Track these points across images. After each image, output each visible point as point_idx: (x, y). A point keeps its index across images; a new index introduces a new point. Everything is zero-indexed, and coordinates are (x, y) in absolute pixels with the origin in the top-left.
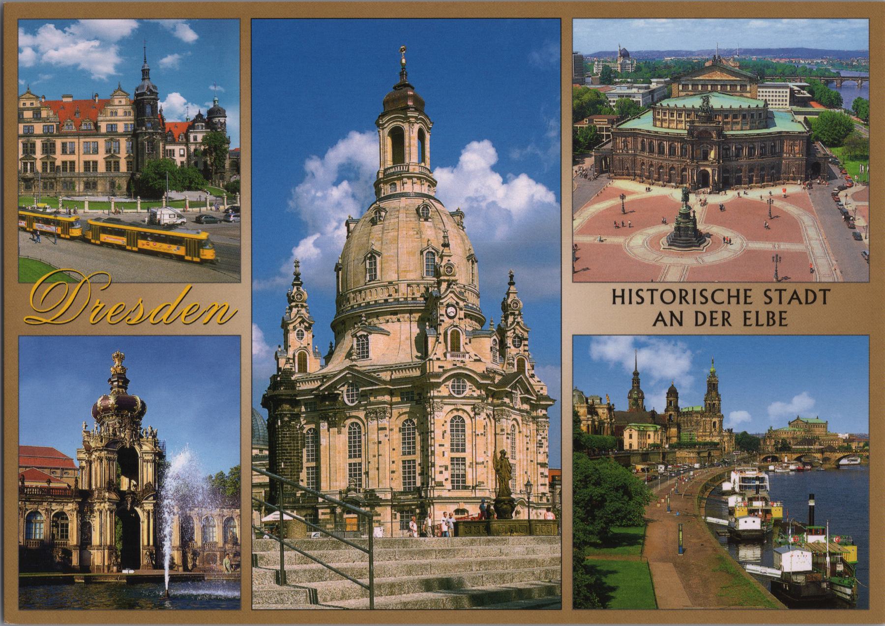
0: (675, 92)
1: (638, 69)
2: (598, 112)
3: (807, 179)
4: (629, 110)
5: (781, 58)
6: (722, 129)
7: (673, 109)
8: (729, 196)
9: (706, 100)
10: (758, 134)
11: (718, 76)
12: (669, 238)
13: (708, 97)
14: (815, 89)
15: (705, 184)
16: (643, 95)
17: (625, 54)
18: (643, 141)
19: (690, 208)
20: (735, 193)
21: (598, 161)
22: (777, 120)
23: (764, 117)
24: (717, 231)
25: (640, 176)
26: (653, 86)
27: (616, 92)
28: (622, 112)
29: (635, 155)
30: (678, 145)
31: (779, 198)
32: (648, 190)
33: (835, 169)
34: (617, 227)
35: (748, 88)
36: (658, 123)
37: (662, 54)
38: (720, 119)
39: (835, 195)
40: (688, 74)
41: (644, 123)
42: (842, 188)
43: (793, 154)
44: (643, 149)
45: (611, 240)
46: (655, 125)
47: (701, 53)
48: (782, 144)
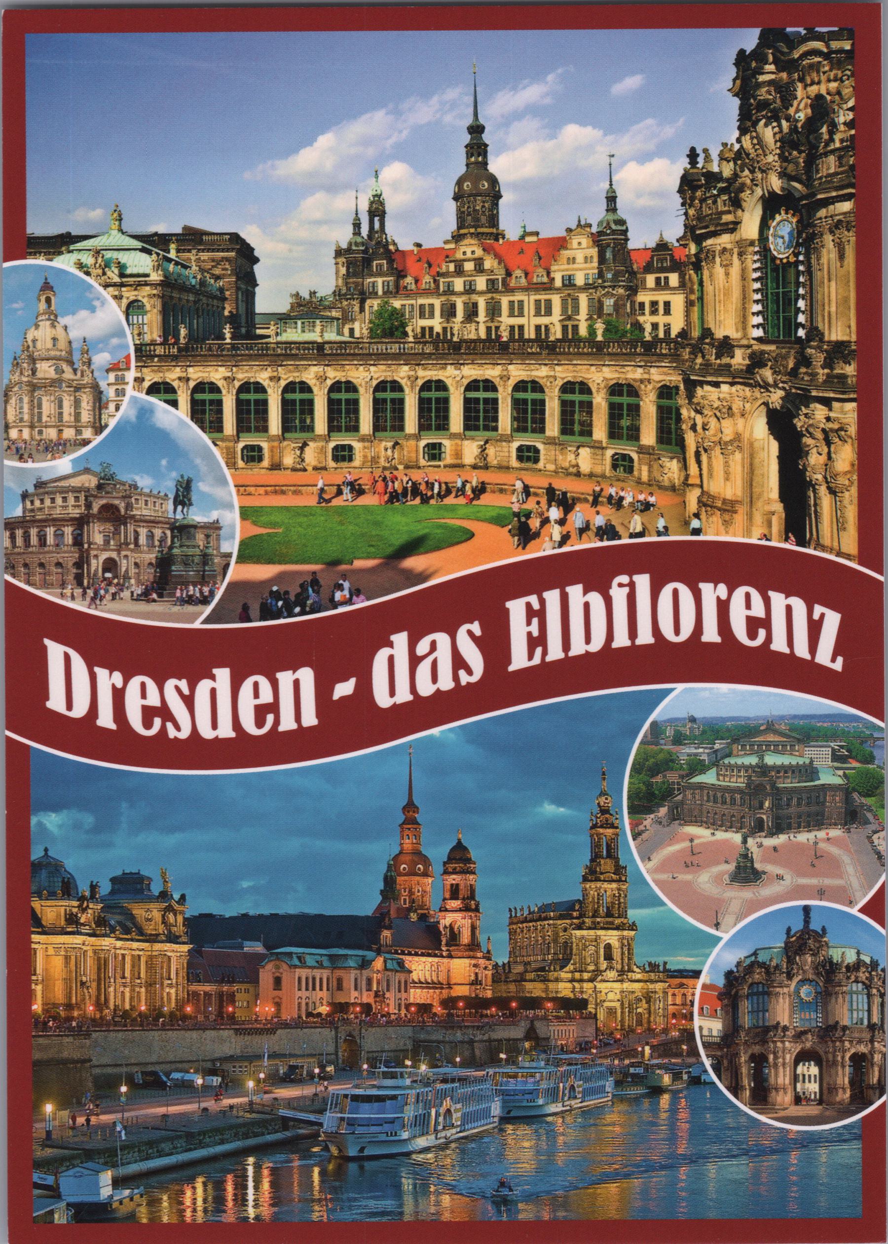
0: (735, 752)
1: (704, 732)
3: (846, 824)
4: (698, 767)
7: (733, 766)
8: (781, 839)
9: (762, 758)
10: (805, 787)
11: (771, 738)
14: (852, 747)
15: (761, 829)
17: (693, 720)
19: (748, 850)
20: (786, 836)
21: (671, 810)
22: (821, 775)
23: (810, 771)
25: (706, 823)
26: (717, 746)
27: (685, 752)
28: (690, 769)
29: (701, 805)
31: (823, 840)
33: (869, 816)
34: (687, 866)
35: (797, 748)
36: (721, 778)
38: (773, 774)
39: (869, 838)
40: (745, 737)
41: (709, 778)
42: (875, 832)
43: (834, 803)
47: (757, 718)
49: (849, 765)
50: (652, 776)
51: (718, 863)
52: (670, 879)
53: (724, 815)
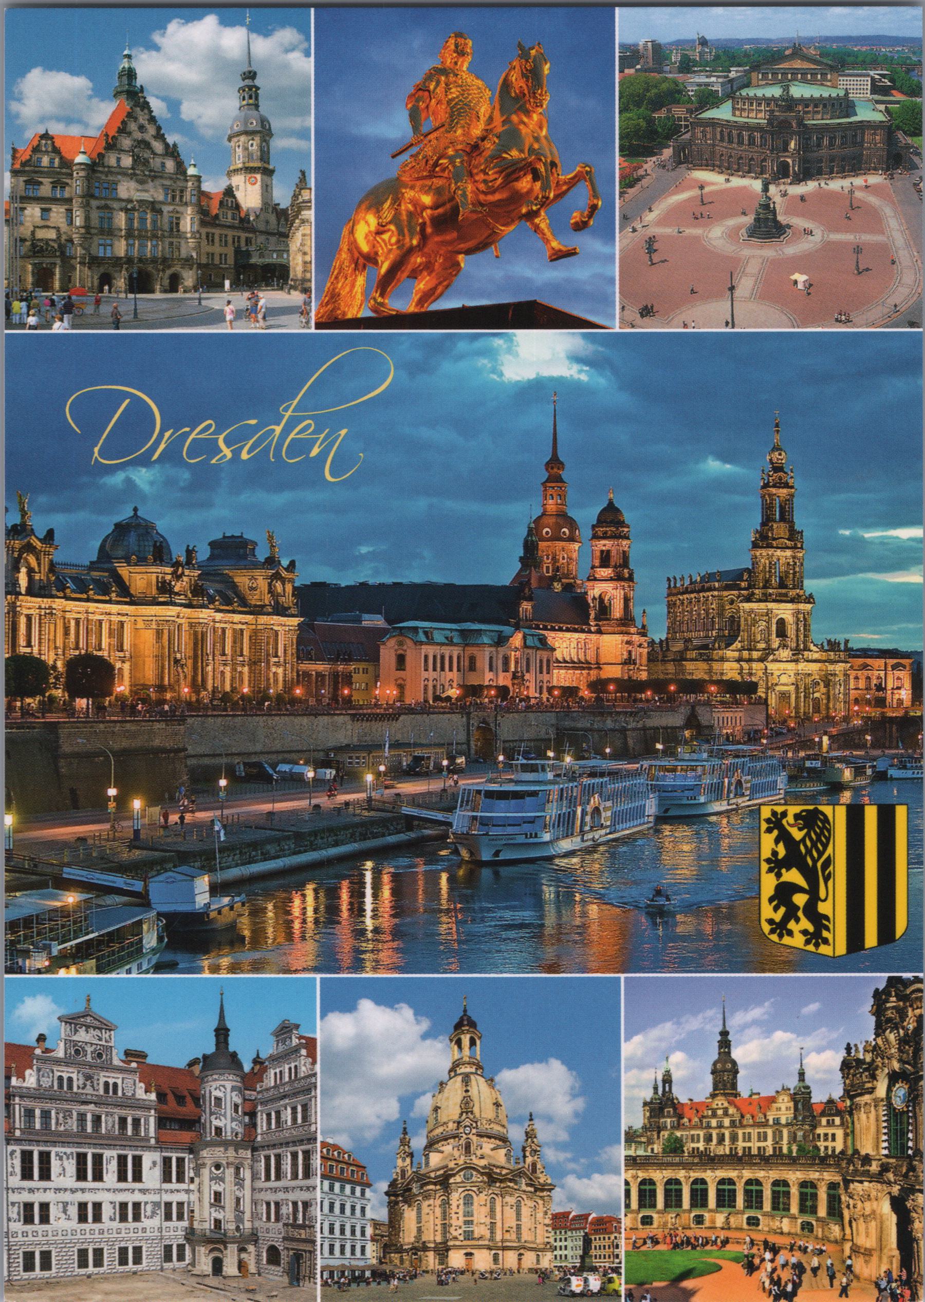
0: (754, 81)
1: (717, 57)
2: (677, 102)
3: (888, 170)
4: (708, 99)
5: (862, 46)
6: (803, 119)
8: (809, 187)
9: (786, 89)
11: (798, 64)
12: (749, 229)
13: (788, 86)
15: (786, 175)
16: (723, 84)
17: (704, 42)
18: (722, 131)
20: (816, 183)
21: (676, 154)
22: (858, 110)
23: (845, 106)
24: (799, 222)
25: (719, 167)
26: (732, 75)
27: (695, 81)
28: (700, 102)
29: (714, 145)
30: (757, 135)
31: (860, 188)
32: (728, 181)
35: (829, 77)
37: (741, 42)
39: (916, 185)
40: (768, 63)
41: (723, 113)
43: (874, 142)
44: (722, 140)
45: (691, 231)
46: (734, 115)
48: (863, 134)
49: (891, 98)
50: (653, 112)
51: (733, 215)
52: (675, 233)
53: (741, 158)
